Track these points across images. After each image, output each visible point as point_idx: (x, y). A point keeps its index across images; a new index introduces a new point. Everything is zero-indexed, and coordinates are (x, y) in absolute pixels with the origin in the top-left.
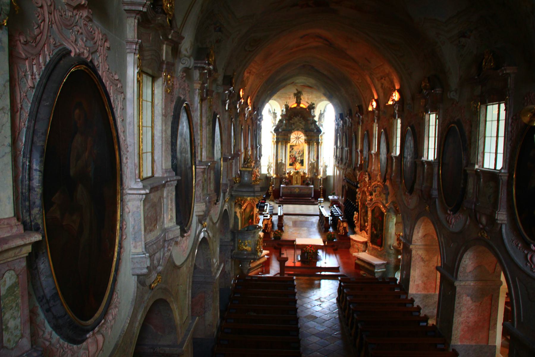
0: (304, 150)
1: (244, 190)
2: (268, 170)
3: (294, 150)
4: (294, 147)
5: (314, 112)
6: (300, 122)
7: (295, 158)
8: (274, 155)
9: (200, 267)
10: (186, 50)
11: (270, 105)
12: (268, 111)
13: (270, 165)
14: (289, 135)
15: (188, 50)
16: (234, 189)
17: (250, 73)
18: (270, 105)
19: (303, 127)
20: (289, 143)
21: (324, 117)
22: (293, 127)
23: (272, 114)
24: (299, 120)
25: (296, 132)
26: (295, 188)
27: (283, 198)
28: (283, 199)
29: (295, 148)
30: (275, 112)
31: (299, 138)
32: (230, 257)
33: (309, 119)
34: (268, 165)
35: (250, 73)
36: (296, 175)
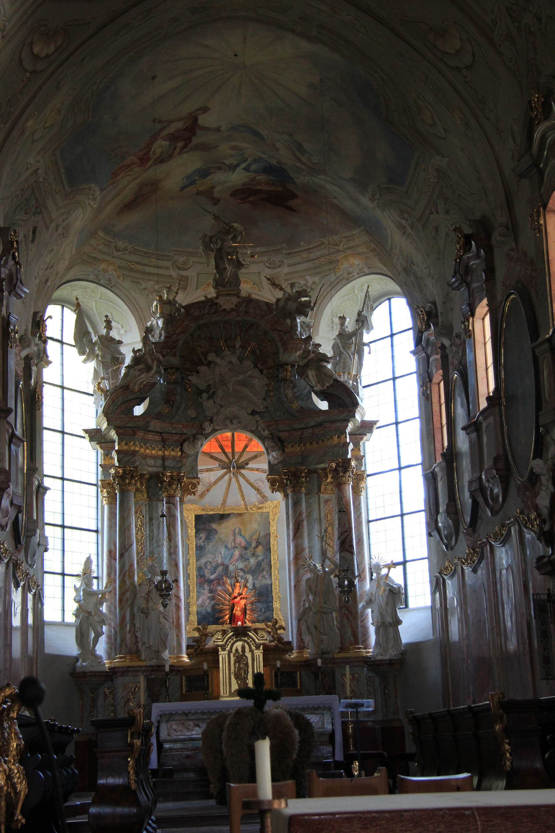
0: (268, 535)
4: (214, 526)
6: (241, 377)
8: (111, 553)
22: (209, 405)
30: (114, 334)
33: (285, 357)
36: (239, 645)
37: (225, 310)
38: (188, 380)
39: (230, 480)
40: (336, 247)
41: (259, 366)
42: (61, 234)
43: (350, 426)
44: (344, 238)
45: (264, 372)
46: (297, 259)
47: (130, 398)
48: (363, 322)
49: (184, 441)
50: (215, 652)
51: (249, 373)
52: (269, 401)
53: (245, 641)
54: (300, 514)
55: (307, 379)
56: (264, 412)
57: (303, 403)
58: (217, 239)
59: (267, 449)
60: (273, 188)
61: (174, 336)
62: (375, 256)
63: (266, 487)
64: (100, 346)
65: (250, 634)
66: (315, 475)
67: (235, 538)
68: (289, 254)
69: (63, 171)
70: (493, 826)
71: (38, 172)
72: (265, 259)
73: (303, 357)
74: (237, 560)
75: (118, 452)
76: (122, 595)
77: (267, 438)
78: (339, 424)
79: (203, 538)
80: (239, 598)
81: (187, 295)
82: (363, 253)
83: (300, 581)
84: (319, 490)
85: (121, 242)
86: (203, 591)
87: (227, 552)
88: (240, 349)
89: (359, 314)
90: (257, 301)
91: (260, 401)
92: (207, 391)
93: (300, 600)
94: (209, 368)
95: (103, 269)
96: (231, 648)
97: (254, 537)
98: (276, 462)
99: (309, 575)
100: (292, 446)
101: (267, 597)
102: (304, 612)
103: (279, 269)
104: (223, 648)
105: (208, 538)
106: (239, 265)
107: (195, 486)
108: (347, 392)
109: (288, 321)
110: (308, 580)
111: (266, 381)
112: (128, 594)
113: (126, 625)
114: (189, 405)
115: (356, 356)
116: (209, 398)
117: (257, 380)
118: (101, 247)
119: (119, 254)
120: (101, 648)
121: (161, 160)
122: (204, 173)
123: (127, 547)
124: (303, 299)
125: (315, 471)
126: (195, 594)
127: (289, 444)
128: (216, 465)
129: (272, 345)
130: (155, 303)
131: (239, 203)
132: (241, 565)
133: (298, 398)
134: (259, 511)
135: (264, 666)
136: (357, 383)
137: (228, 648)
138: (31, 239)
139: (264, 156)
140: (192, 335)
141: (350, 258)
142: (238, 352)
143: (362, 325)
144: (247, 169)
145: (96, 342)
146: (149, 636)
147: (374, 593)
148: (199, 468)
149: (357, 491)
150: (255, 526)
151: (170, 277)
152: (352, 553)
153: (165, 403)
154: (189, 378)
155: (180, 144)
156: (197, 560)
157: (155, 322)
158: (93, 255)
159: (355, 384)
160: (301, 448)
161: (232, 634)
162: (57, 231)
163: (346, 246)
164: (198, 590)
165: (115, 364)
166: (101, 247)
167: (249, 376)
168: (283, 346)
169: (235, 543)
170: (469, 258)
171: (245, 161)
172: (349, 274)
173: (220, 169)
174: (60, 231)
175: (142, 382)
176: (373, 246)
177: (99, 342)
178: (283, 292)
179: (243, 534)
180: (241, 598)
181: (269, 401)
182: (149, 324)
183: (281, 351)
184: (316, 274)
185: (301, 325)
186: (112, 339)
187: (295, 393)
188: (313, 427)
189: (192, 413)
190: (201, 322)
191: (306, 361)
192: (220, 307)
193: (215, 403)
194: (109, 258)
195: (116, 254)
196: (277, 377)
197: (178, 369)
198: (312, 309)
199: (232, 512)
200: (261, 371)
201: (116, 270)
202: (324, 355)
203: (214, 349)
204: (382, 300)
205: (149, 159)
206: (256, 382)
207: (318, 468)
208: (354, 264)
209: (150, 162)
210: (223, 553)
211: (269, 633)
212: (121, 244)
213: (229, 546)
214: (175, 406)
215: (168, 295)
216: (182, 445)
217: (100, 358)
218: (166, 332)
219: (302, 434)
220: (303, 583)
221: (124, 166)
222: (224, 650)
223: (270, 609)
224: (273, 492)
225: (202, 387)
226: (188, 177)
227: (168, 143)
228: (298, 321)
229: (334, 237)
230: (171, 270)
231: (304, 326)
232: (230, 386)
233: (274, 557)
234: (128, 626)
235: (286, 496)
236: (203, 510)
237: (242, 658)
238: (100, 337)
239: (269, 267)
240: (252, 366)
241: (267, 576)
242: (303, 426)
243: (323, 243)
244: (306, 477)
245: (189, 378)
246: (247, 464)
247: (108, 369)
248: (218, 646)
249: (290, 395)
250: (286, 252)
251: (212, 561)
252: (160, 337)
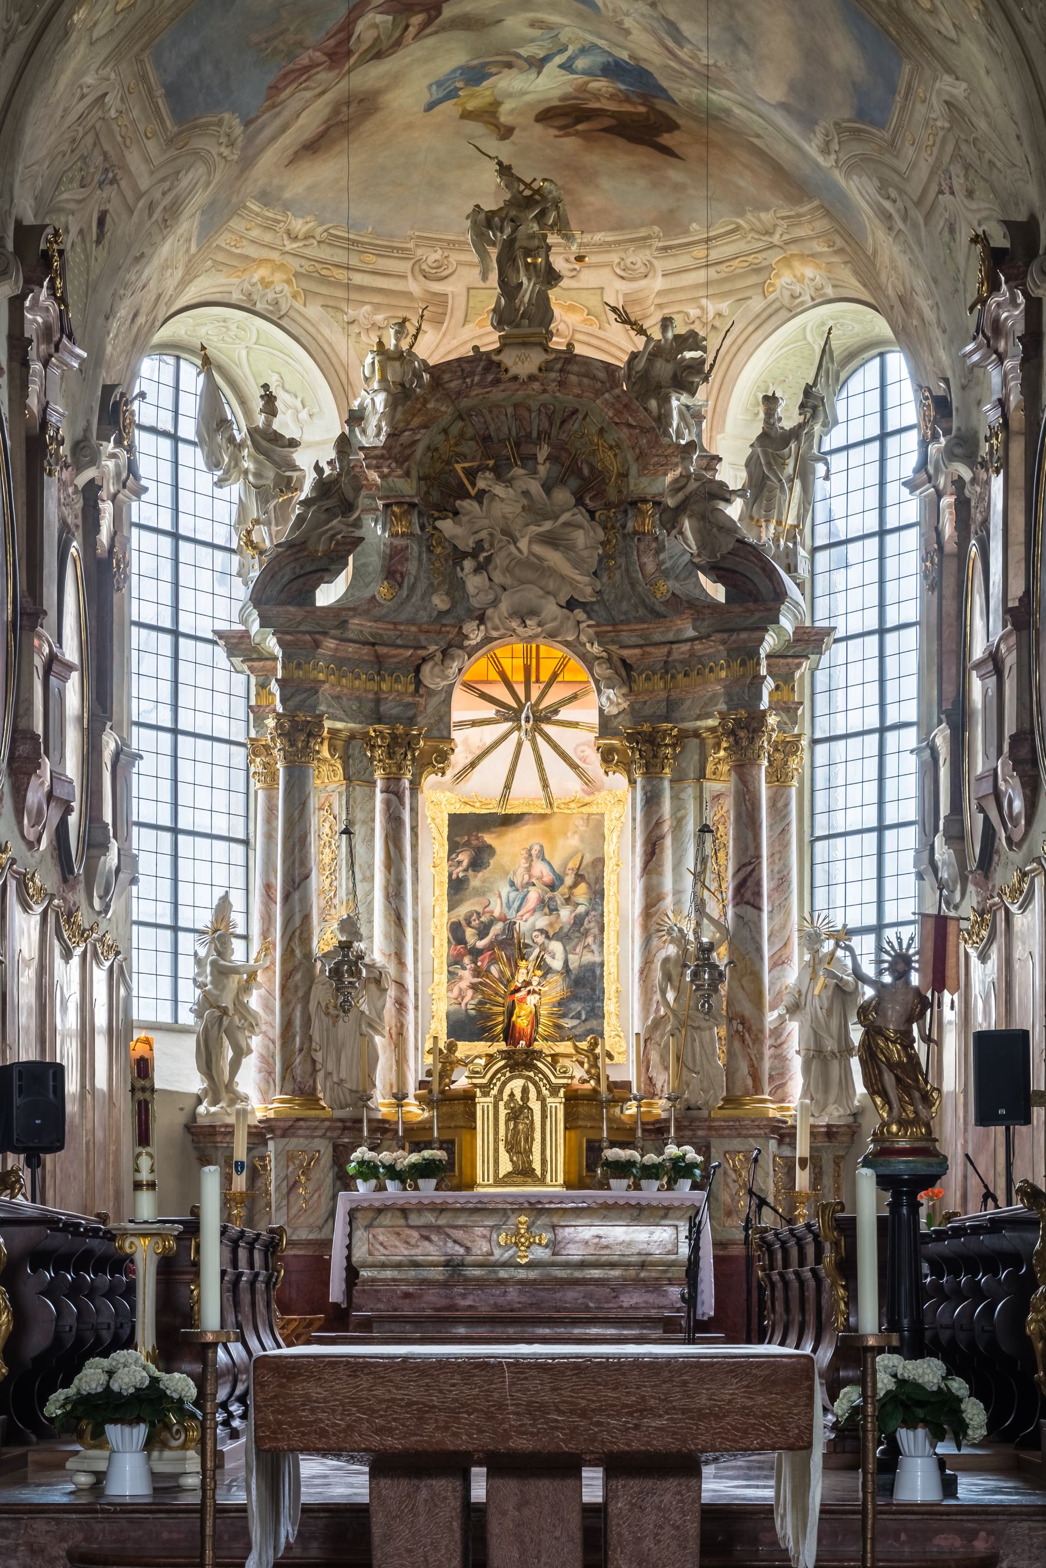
0: (599, 862)
4: (488, 838)
6: (547, 526)
13: (227, 1001)
14: (428, 674)
19: (585, 587)
22: (474, 583)
24: (534, 512)
36: (516, 1085)
37: (515, 378)
38: (435, 528)
39: (520, 745)
40: (766, 238)
41: (587, 501)
42: (160, 220)
43: (770, 642)
44: (783, 218)
45: (597, 514)
46: (684, 260)
47: (309, 568)
48: (815, 408)
49: (424, 660)
50: (468, 1098)
51: (565, 517)
52: (605, 579)
53: (529, 1078)
54: (659, 824)
55: (680, 537)
56: (593, 603)
57: (677, 585)
58: (502, 220)
59: (597, 682)
60: (627, 108)
61: (407, 433)
62: (846, 263)
63: (593, 763)
64: (252, 450)
65: (540, 1064)
66: (696, 741)
67: (530, 866)
68: (665, 249)
69: (159, 92)
70: (526, 1379)
71: (107, 99)
72: (615, 258)
73: (677, 487)
74: (534, 910)
75: (282, 683)
76: (286, 977)
77: (598, 658)
78: (744, 635)
79: (465, 864)
80: (523, 992)
81: (444, 335)
82: (821, 253)
83: (652, 962)
84: (702, 775)
85: (300, 221)
86: (461, 972)
87: (513, 895)
88: (548, 465)
89: (808, 391)
90: (587, 361)
91: (587, 579)
92: (474, 555)
93: (651, 1000)
94: (481, 503)
95: (262, 280)
96: (501, 1091)
97: (570, 865)
98: (615, 711)
99: (672, 950)
100: (648, 679)
101: (593, 989)
102: (657, 1024)
103: (643, 283)
104: (485, 1089)
105: (477, 864)
106: (552, 277)
107: (444, 757)
108: (764, 570)
109: (653, 404)
110: (666, 960)
111: (601, 535)
112: (298, 976)
113: (294, 1037)
114: (436, 582)
115: (797, 485)
116: (479, 569)
117: (581, 532)
118: (255, 233)
119: (295, 245)
121: (377, 54)
122: (475, 75)
123: (297, 880)
124: (689, 355)
125: (696, 734)
126: (444, 977)
127: (640, 674)
128: (489, 711)
129: (615, 455)
130: (369, 360)
131: (556, 136)
132: (542, 922)
133: (666, 574)
134: (584, 810)
135: (566, 1128)
136: (795, 543)
137: (494, 1092)
138: (94, 238)
139: (601, 43)
140: (445, 431)
141: (796, 264)
142: (542, 470)
143: (814, 416)
144: (567, 67)
145: (243, 441)
146: (339, 1060)
147: (804, 992)
148: (456, 716)
149: (779, 776)
150: (574, 841)
151: (408, 295)
152: (759, 909)
153: (386, 578)
154: (439, 524)
155: (417, 20)
156: (451, 908)
157: (368, 401)
158: (238, 251)
159: (791, 545)
160: (666, 683)
161: (503, 1063)
162: (150, 216)
163: (786, 237)
164: (451, 969)
165: (282, 491)
166: (255, 233)
167: (566, 524)
168: (637, 460)
169: (530, 877)
170: (999, 305)
171: (561, 51)
172: (793, 297)
173: (509, 65)
174: (157, 215)
175: (333, 537)
176: (839, 242)
177: (249, 443)
178: (644, 338)
179: (547, 857)
180: (529, 992)
181: (605, 579)
182: (355, 405)
183: (634, 470)
184: (723, 295)
185: (681, 415)
186: (276, 438)
187: (663, 562)
188: (692, 640)
189: (440, 602)
190: (465, 403)
191: (681, 496)
192: (506, 371)
193: (490, 579)
194: (275, 255)
195: (290, 246)
196: (624, 527)
197: (413, 505)
198: (706, 379)
199: (525, 810)
200: (592, 514)
201: (288, 282)
202: (722, 485)
203: (491, 463)
204: (866, 355)
205: (349, 53)
206: (580, 538)
207: (700, 728)
208: (803, 275)
209: (353, 60)
210: (504, 895)
211: (582, 1064)
212: (299, 225)
213: (518, 881)
214: (405, 585)
215: (398, 340)
216: (417, 670)
217: (251, 478)
218: (391, 423)
219: (669, 653)
220: (657, 964)
221: (293, 71)
222: (486, 1094)
223: (596, 1013)
224: (607, 773)
225: (467, 544)
226: (439, 84)
227: (391, 18)
228: (675, 403)
229: (763, 215)
230: (410, 278)
231: (688, 415)
232: (523, 544)
233: (610, 906)
234: (298, 1039)
235: (632, 782)
236: (466, 803)
237: (521, 1112)
238: (253, 432)
239: (622, 278)
240: (573, 501)
241: (594, 947)
242: (670, 636)
243: (737, 229)
244: (674, 746)
245: (439, 524)
246: (556, 712)
247: (267, 502)
248: (475, 1085)
249: (651, 567)
250: (661, 244)
251: (480, 910)
252: (378, 435)
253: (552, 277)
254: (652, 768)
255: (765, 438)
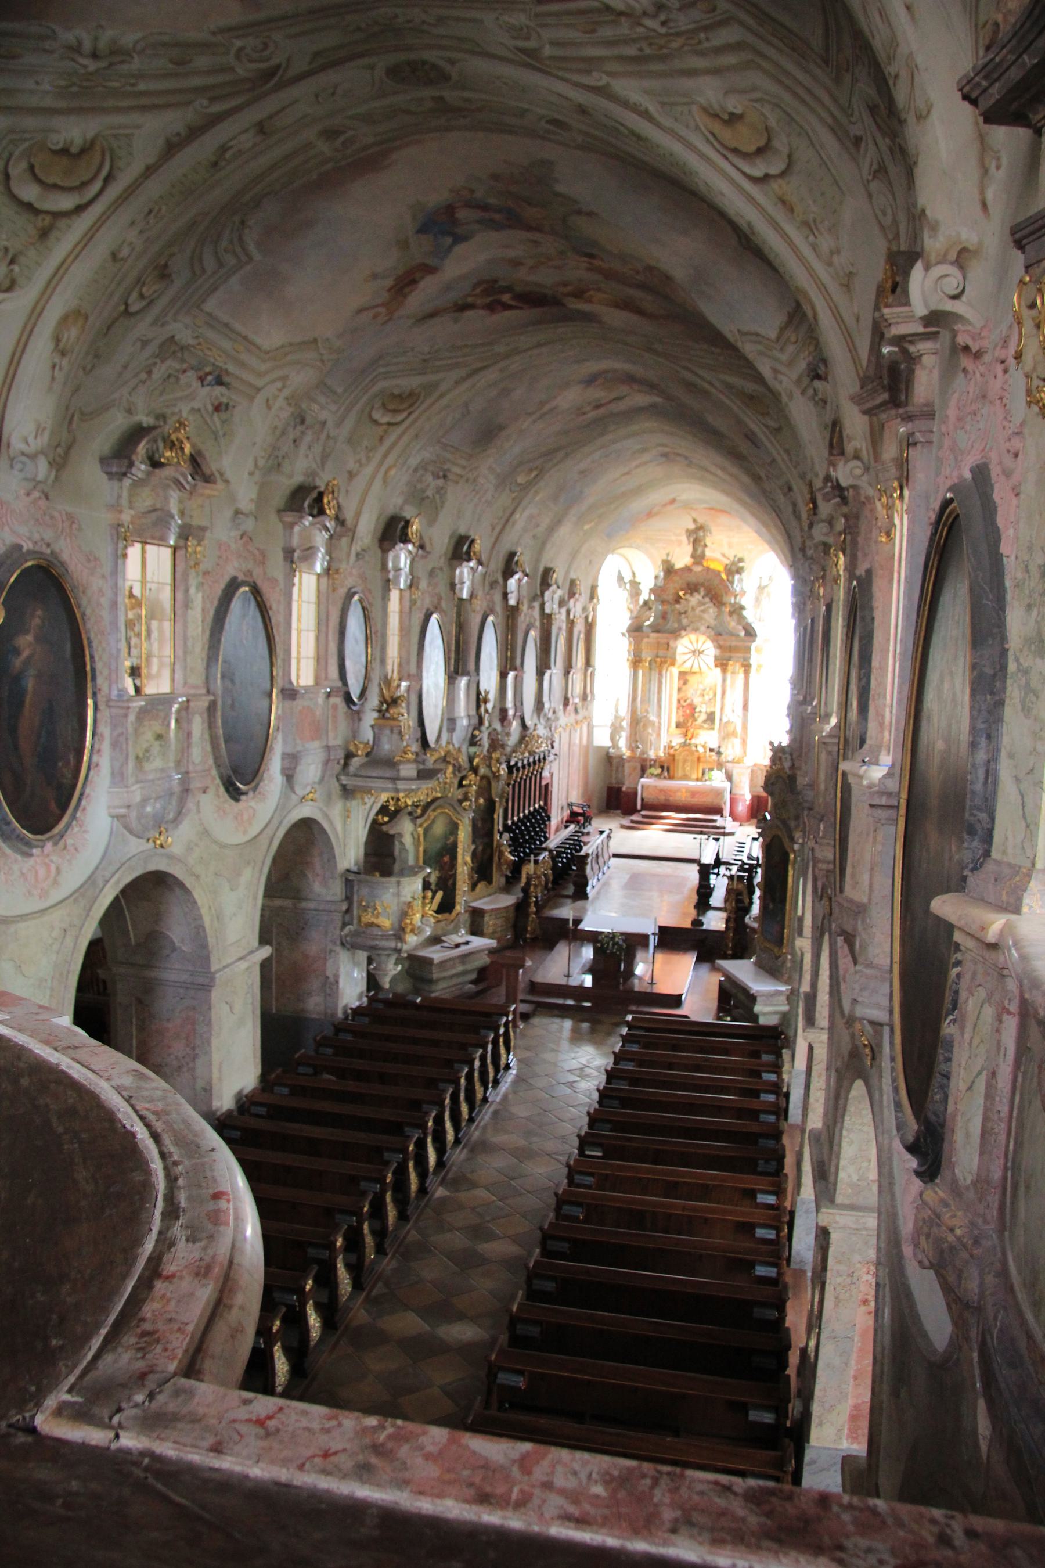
1: (374, 774)
2: (612, 739)
3: (689, 684)
5: (741, 580)
7: (693, 708)
9: (184, 948)
10: (26, 442)
11: (627, 559)
12: (616, 578)
14: (671, 644)
15: (31, 439)
16: (352, 769)
17: (445, 477)
18: (627, 559)
20: (673, 664)
21: (768, 595)
22: (685, 621)
23: (628, 586)
24: (701, 604)
25: (693, 637)
26: (679, 790)
27: (643, 813)
28: (644, 816)
29: (692, 680)
30: (638, 580)
31: (701, 653)
32: (338, 942)
34: (613, 725)
35: (445, 477)
120: (622, 743)
253: (706, 546)
254: (724, 671)
255: (759, 587)
